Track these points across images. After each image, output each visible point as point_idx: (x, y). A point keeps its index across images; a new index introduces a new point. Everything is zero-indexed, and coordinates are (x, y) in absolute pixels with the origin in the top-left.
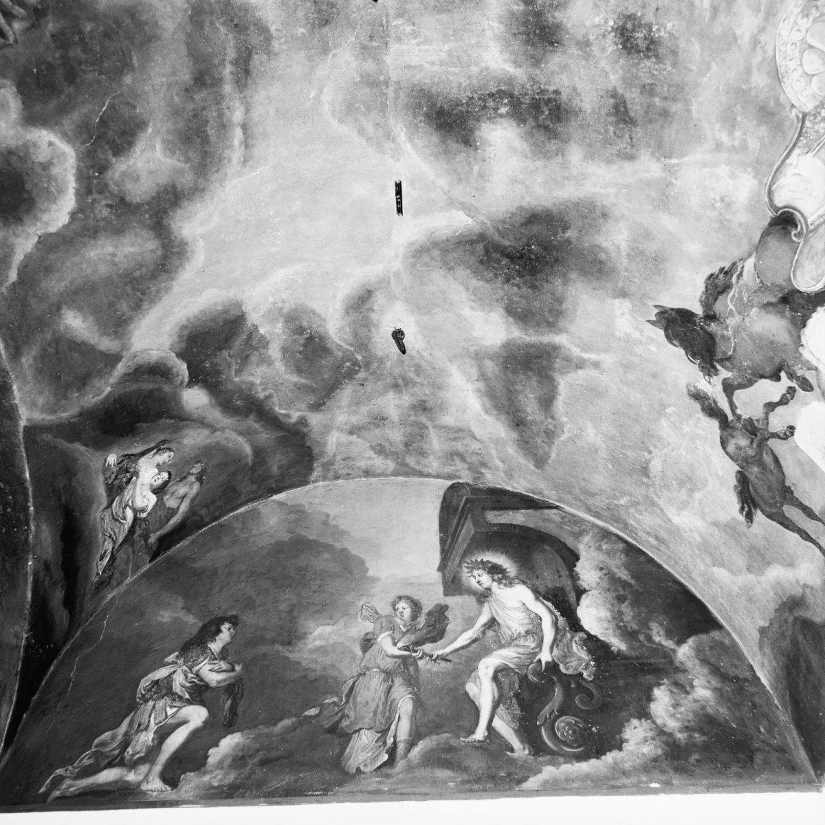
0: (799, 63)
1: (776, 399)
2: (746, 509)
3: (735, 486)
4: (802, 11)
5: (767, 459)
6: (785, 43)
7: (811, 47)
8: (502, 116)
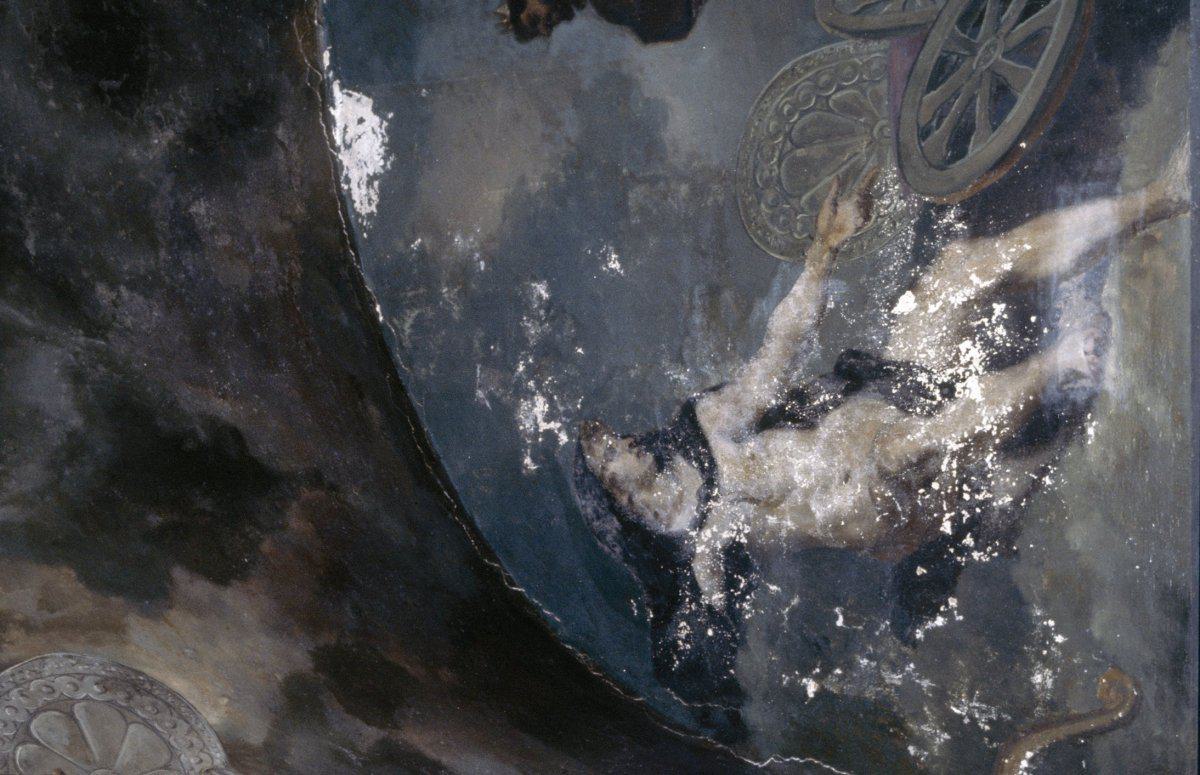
0: (32, 709)
4: (106, 679)
6: (39, 675)
7: (71, 716)
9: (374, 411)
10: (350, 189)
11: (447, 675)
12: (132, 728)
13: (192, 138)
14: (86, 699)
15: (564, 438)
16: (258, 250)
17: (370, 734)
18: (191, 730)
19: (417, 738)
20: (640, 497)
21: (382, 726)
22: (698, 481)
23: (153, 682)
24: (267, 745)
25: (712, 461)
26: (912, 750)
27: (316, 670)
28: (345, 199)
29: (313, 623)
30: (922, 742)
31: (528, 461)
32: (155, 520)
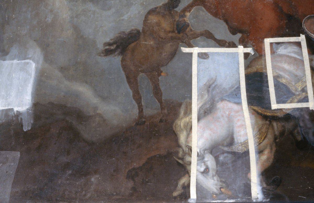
1: (218, 37)
2: (112, 48)
3: (124, 32)
5: (168, 48)
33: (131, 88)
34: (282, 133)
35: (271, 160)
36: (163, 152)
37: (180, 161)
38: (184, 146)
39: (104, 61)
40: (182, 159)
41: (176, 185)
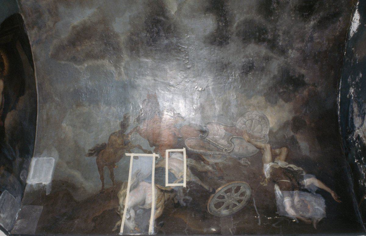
0: (248, 119)
1: (144, 148)
2: (93, 152)
4: (260, 116)
7: (252, 122)
8: (218, 23)
9: (333, 72)
10: (351, 30)
11: (313, 125)
12: (259, 125)
13: (320, 22)
14: (256, 119)
15: (352, 98)
16: (325, 42)
17: (292, 133)
18: (267, 127)
19: (298, 137)
20: (355, 117)
21: (295, 133)
22: (361, 124)
23: (266, 118)
24: (275, 132)
25: (363, 123)
26: (359, 181)
27: (292, 120)
28: (349, 31)
29: (296, 112)
30: (361, 181)
31: (348, 95)
32: (281, 90)
33: (100, 173)
34: (168, 199)
35: (161, 213)
36: (110, 208)
37: (118, 213)
38: (121, 205)
39: (88, 159)
40: (119, 212)
41: (115, 225)
